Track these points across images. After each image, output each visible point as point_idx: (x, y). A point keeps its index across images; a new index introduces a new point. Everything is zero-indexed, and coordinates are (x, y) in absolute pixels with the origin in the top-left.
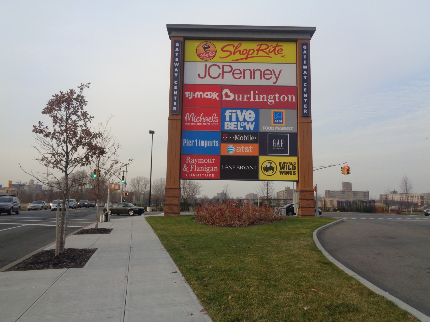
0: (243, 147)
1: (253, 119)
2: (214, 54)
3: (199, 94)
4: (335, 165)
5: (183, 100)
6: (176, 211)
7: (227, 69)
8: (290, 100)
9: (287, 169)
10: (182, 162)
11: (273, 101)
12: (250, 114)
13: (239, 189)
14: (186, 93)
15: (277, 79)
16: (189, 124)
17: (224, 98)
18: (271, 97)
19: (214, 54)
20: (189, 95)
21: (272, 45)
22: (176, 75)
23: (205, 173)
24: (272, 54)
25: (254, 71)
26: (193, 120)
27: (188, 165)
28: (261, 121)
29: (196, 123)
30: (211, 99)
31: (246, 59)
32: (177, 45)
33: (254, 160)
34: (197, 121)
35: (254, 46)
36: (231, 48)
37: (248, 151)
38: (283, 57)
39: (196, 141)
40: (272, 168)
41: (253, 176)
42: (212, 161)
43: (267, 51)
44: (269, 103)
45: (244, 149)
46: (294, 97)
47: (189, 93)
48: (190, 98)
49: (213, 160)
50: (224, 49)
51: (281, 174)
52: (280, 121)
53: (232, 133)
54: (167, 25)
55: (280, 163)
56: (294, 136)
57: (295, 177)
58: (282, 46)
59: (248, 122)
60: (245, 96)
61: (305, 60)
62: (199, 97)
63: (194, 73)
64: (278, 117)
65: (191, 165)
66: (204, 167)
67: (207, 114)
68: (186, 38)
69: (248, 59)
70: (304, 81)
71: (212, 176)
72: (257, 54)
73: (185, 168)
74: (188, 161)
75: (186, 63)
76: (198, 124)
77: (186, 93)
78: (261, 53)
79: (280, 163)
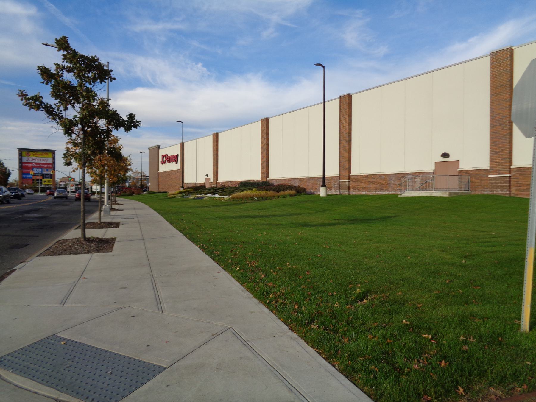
20: (24, 165)
63: (25, 159)
64: (47, 170)
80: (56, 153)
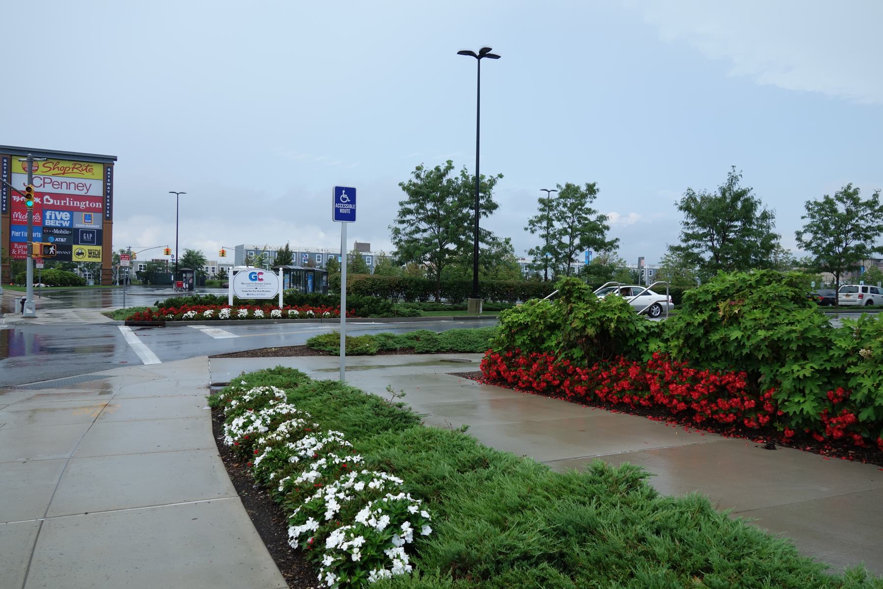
7: (47, 181)
24: (84, 172)
27: (16, 249)
35: (70, 165)
36: (51, 165)
40: (82, 253)
53: (51, 228)
56: (100, 232)
64: (88, 218)
70: (108, 194)
73: (14, 252)
78: (75, 170)
80: (118, 168)
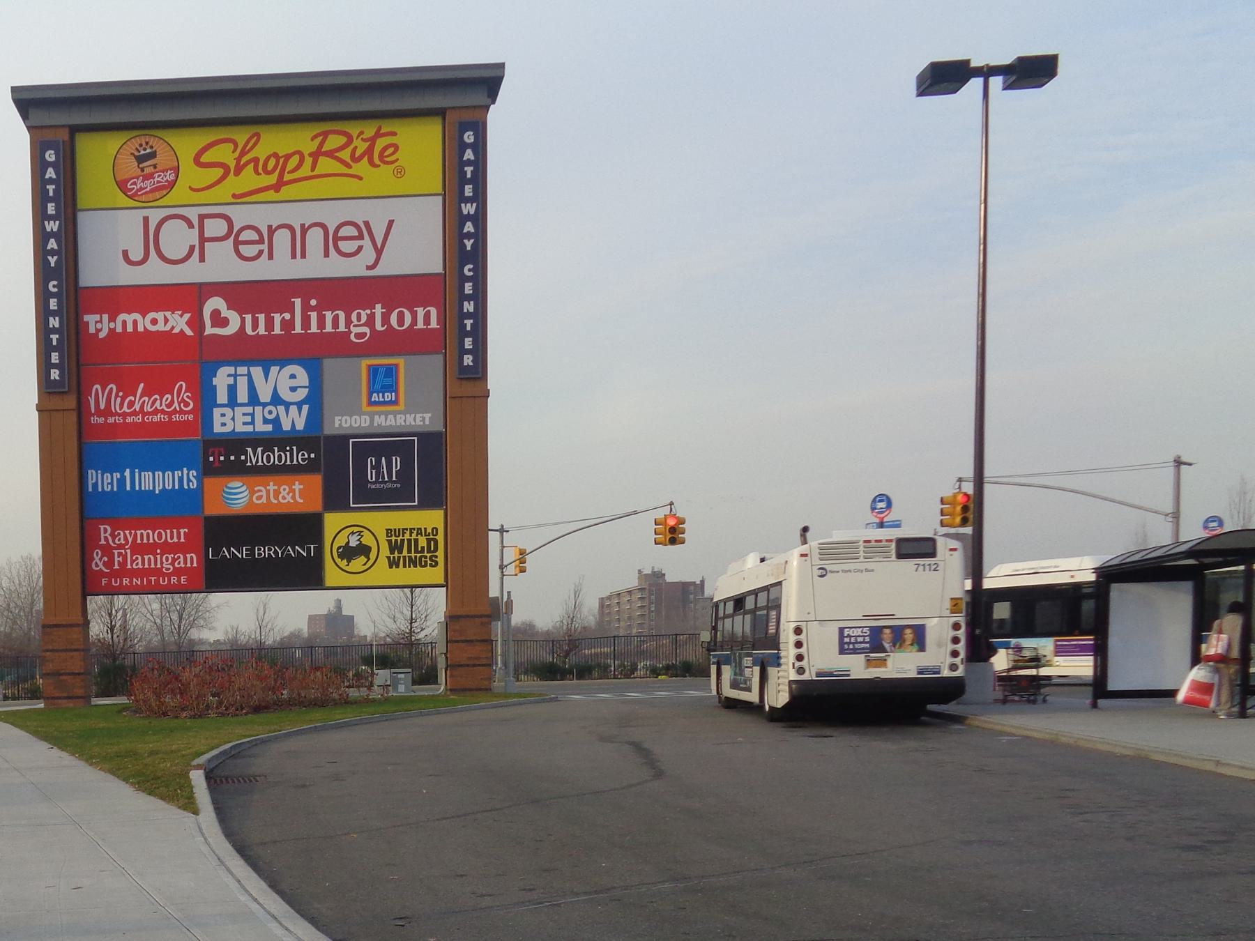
0: (272, 487)
1: (302, 394)
2: (170, 176)
3: (129, 318)
4: (635, 513)
5: (84, 346)
6: (80, 692)
7: (215, 228)
8: (420, 325)
9: (409, 551)
10: (87, 542)
11: (366, 330)
12: (293, 376)
13: (284, 614)
14: (87, 318)
15: (379, 252)
16: (101, 420)
17: (209, 330)
18: (359, 316)
19: (172, 177)
20: (98, 324)
21: (362, 133)
22: (53, 260)
23: (158, 572)
24: (362, 167)
25: (304, 230)
26: (115, 406)
27: (107, 550)
28: (328, 400)
29: (124, 415)
30: (169, 333)
31: (277, 187)
32: (50, 156)
33: (305, 527)
34: (125, 409)
35: (300, 139)
36: (225, 154)
37: (289, 499)
38: (400, 172)
39: (127, 473)
40: (364, 550)
41: (307, 575)
42: (179, 534)
43: (345, 155)
44: (352, 337)
45: (277, 493)
46: (433, 311)
47: (97, 317)
48: (102, 335)
49: (182, 531)
50: (205, 158)
51: (391, 567)
52: (389, 396)
53: (237, 444)
54: (15, 90)
55: (389, 532)
56: (432, 442)
57: (437, 574)
58: (394, 134)
59: (287, 405)
60: (277, 318)
61: (469, 182)
62: (130, 329)
63: (113, 248)
64: (383, 381)
65: (116, 552)
66: (155, 554)
67: (159, 387)
68: (75, 130)
69: (284, 189)
71: (179, 580)
72: (313, 168)
73: (98, 562)
74: (106, 539)
75: (82, 217)
76: (129, 420)
77: (87, 318)
78: (326, 164)
79: (389, 532)
80: (498, 118)
